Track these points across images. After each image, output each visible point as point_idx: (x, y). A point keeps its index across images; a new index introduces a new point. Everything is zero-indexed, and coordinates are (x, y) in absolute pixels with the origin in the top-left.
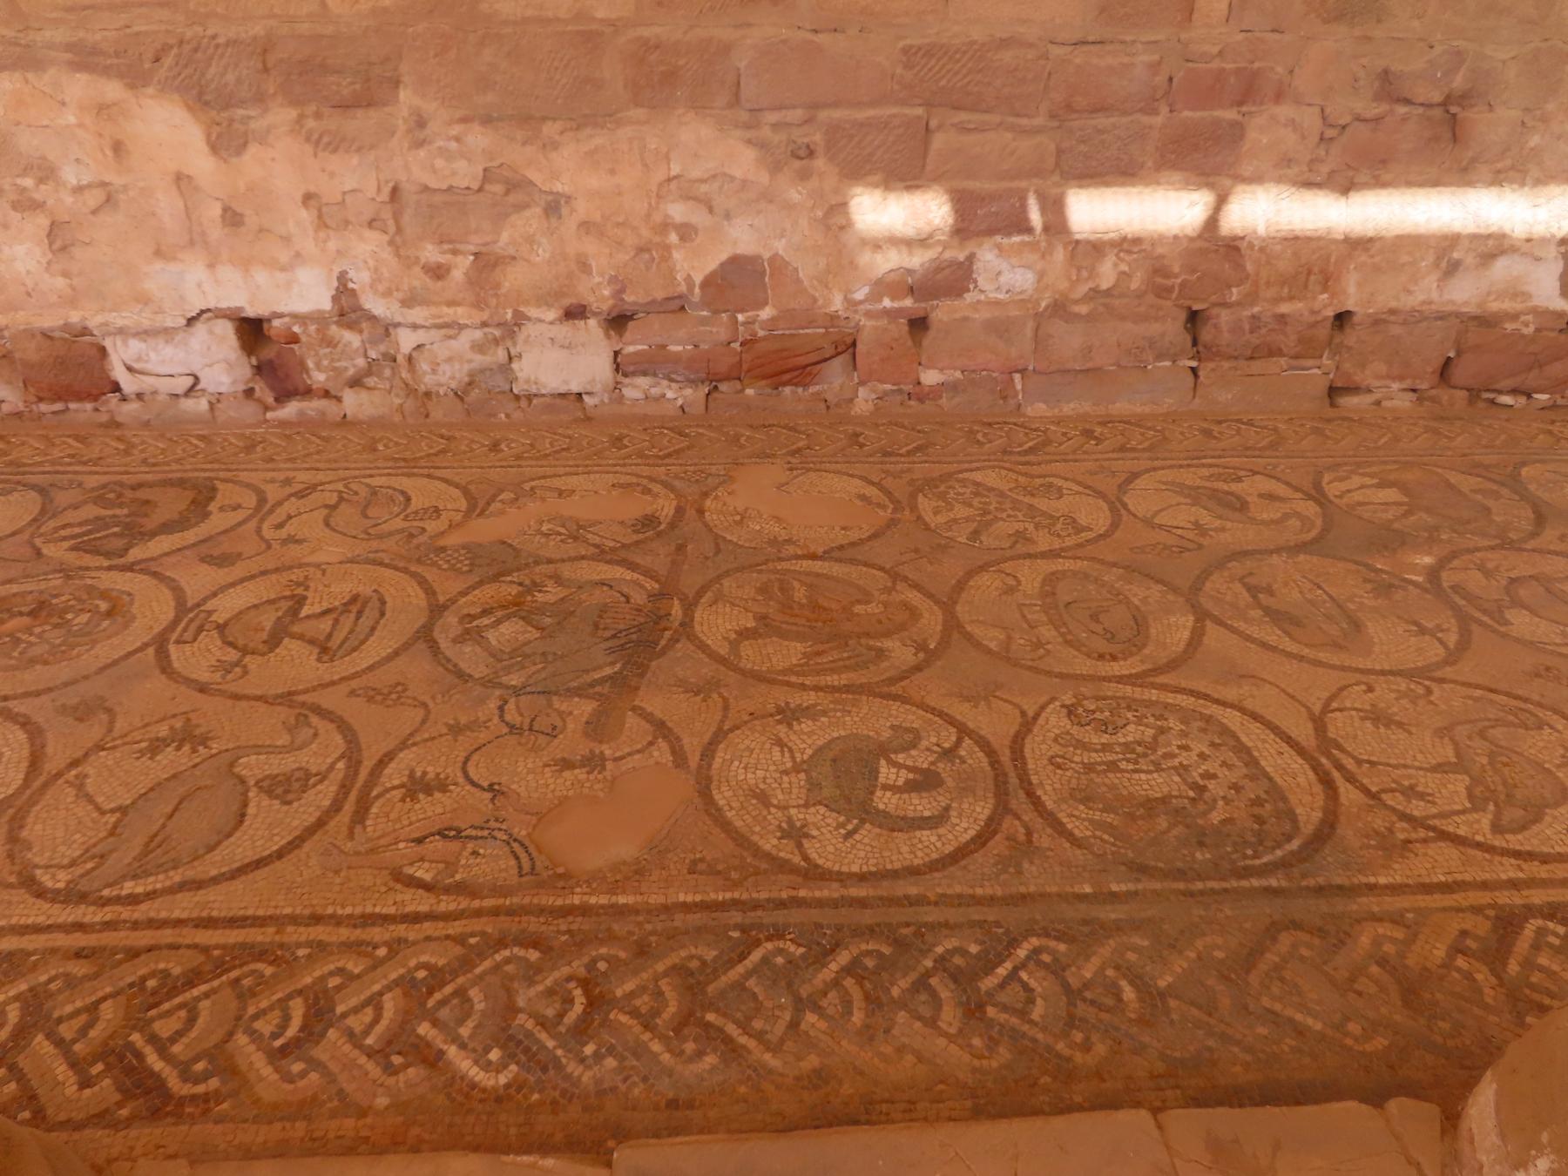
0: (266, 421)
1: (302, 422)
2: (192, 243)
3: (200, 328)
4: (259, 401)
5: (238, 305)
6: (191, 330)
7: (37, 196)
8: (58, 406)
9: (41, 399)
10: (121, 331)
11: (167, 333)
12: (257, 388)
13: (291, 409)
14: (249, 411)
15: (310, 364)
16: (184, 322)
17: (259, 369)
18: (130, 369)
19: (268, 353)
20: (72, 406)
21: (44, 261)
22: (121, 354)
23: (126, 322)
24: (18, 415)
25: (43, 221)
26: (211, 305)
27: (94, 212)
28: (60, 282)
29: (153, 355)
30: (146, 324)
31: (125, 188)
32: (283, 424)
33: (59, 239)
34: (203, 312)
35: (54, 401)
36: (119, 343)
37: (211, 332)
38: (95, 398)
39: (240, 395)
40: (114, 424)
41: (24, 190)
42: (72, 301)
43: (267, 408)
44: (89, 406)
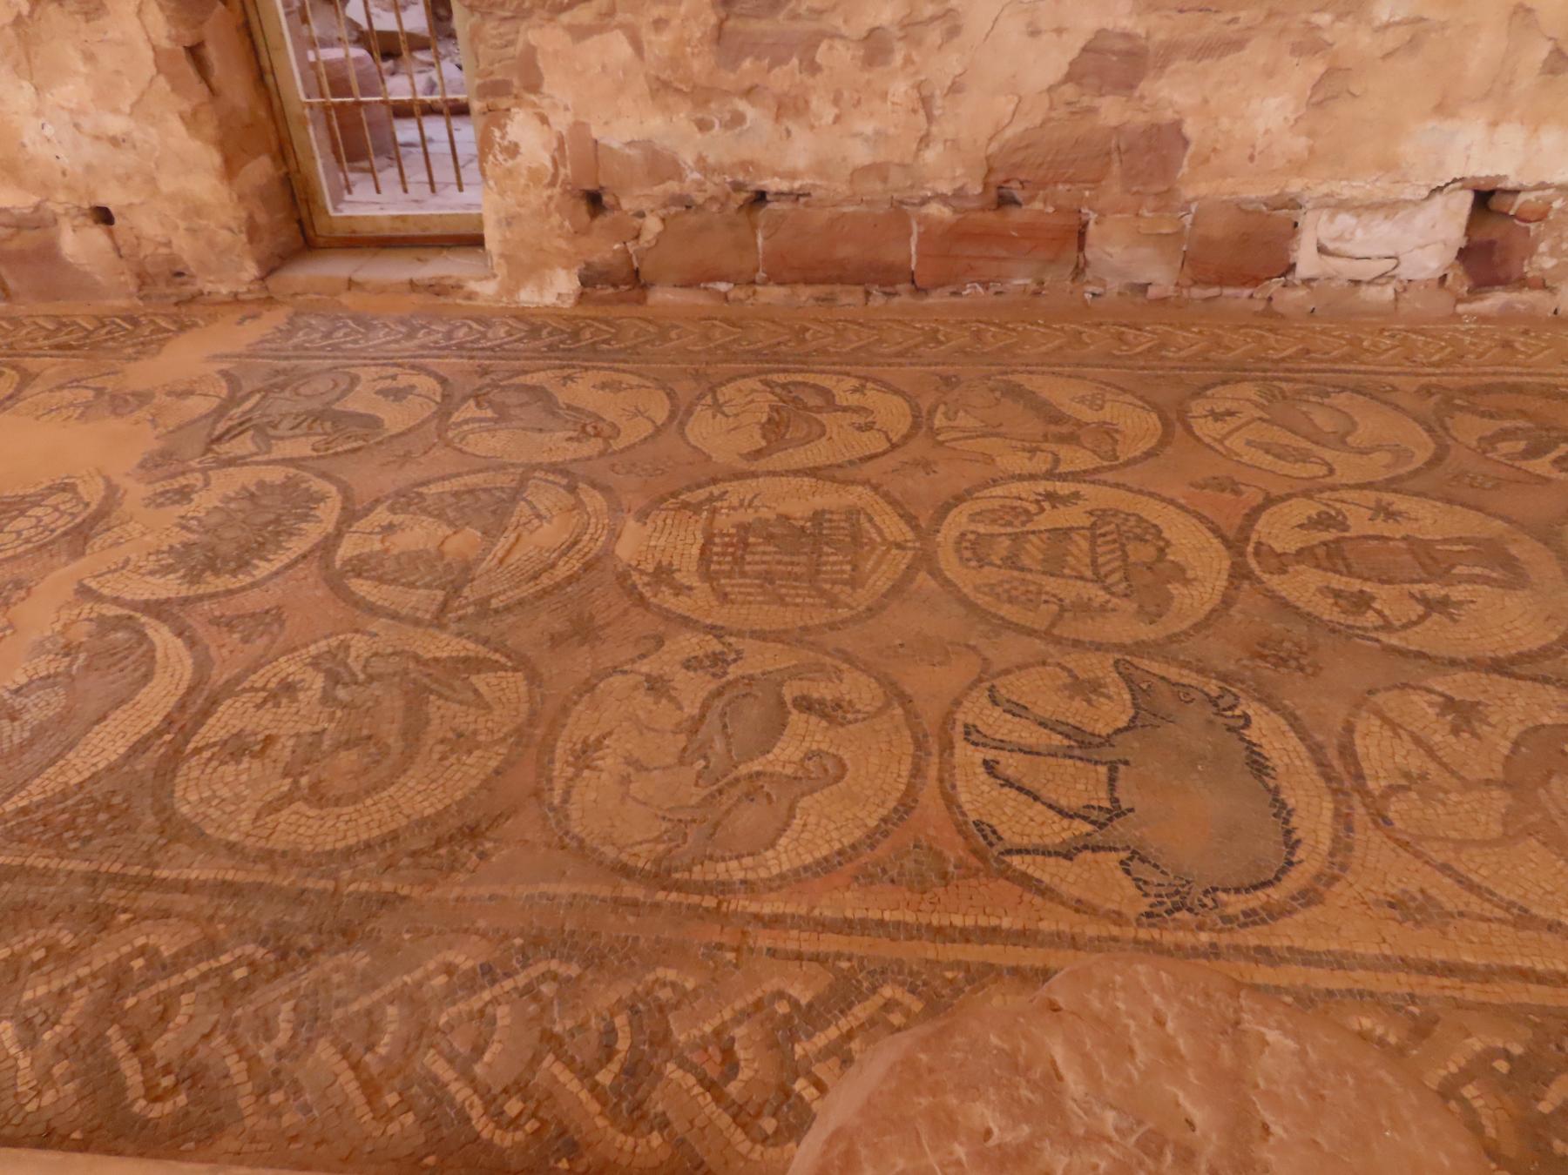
0: (1457, 317)
1: (1506, 316)
2: (1487, 95)
3: (1439, 199)
4: (1449, 289)
5: (1502, 173)
6: (1427, 203)
7: (1327, 37)
8: (1214, 291)
9: (1195, 283)
10: (1342, 206)
11: (1388, 207)
12: (1450, 278)
13: (1495, 300)
14: (1442, 301)
15: (1543, 247)
16: (1425, 193)
17: (1463, 254)
18: (1322, 250)
19: (1493, 230)
20: (1228, 291)
21: (1292, 117)
22: (1316, 228)
23: (1355, 193)
24: (1163, 300)
25: (1318, 68)
26: (1469, 174)
27: (1387, 56)
28: (1300, 144)
29: (1359, 234)
30: (1379, 196)
31: (1444, 26)
32: (1483, 319)
33: (1325, 94)
34: (1455, 181)
35: (1209, 284)
36: (1324, 217)
37: (1445, 206)
38: (1255, 281)
39: (1435, 283)
40: (1269, 312)
41: (1319, 28)
42: (1298, 167)
43: (1459, 301)
44: (1247, 292)
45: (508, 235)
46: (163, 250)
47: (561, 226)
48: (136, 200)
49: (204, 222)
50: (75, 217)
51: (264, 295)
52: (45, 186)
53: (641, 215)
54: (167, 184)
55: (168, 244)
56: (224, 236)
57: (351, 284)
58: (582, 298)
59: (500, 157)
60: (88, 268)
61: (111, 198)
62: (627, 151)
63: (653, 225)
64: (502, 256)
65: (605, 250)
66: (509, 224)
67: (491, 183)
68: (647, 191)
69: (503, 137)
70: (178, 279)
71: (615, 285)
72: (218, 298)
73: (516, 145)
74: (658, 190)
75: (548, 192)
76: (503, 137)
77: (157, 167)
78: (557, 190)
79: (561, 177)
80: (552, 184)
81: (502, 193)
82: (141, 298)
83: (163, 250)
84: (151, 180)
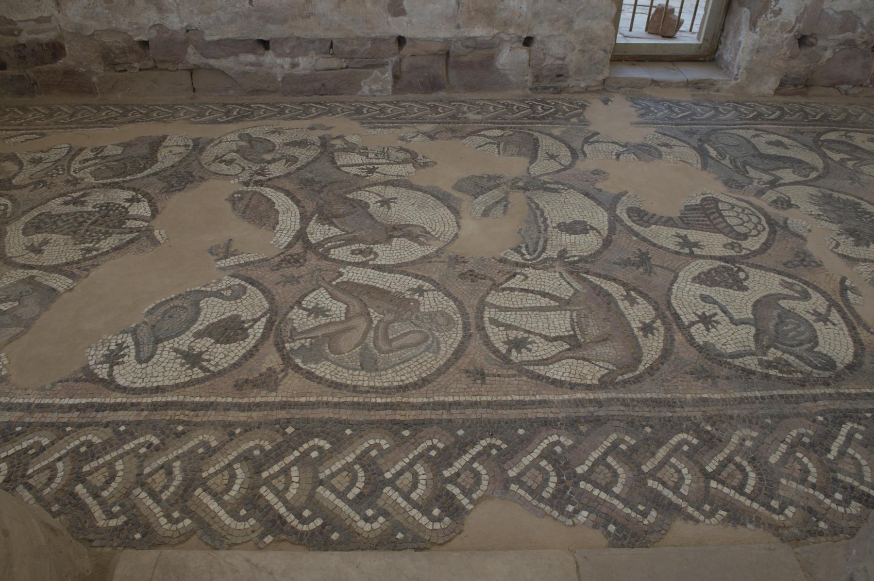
45: (754, 58)
46: (560, 62)
47: (785, 54)
48: (555, 33)
49: (591, 47)
50: (513, 43)
51: (601, 88)
52: (506, 24)
53: (825, 49)
54: (579, 24)
55: (563, 59)
56: (601, 54)
57: (655, 83)
58: (777, 92)
59: (769, 16)
60: (508, 72)
61: (540, 31)
62: (836, 16)
63: (828, 54)
64: (746, 68)
65: (799, 66)
66: (758, 52)
67: (758, 30)
68: (837, 37)
69: (775, 6)
70: (557, 79)
71: (796, 86)
72: (576, 89)
73: (780, 10)
74: (841, 37)
75: (786, 35)
76: (775, 6)
77: (578, 13)
78: (792, 34)
79: (797, 28)
80: (790, 32)
81: (761, 36)
82: (531, 89)
83: (560, 62)
84: (570, 22)
